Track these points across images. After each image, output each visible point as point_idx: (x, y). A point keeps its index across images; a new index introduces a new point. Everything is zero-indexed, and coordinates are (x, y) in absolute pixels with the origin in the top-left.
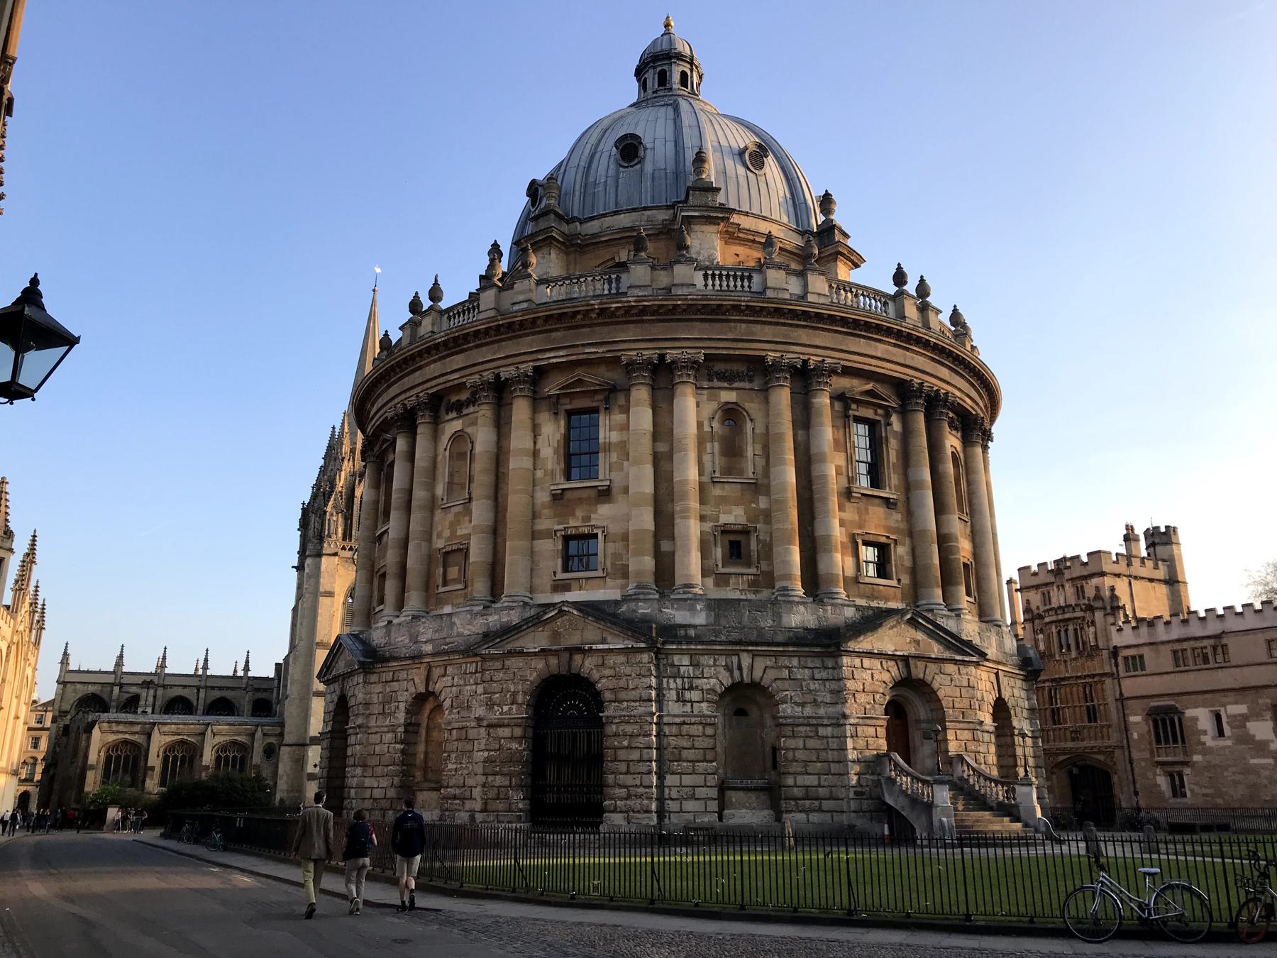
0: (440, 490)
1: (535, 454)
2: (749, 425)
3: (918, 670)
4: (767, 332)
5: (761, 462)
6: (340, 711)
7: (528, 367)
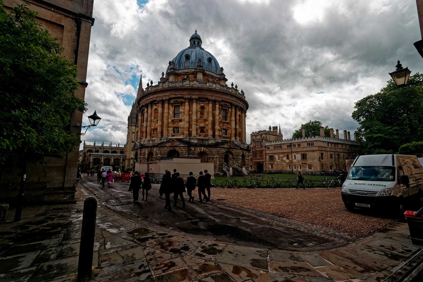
0: (152, 118)
1: (169, 113)
2: (205, 110)
4: (209, 94)
5: (207, 116)
6: (136, 154)
7: (167, 98)
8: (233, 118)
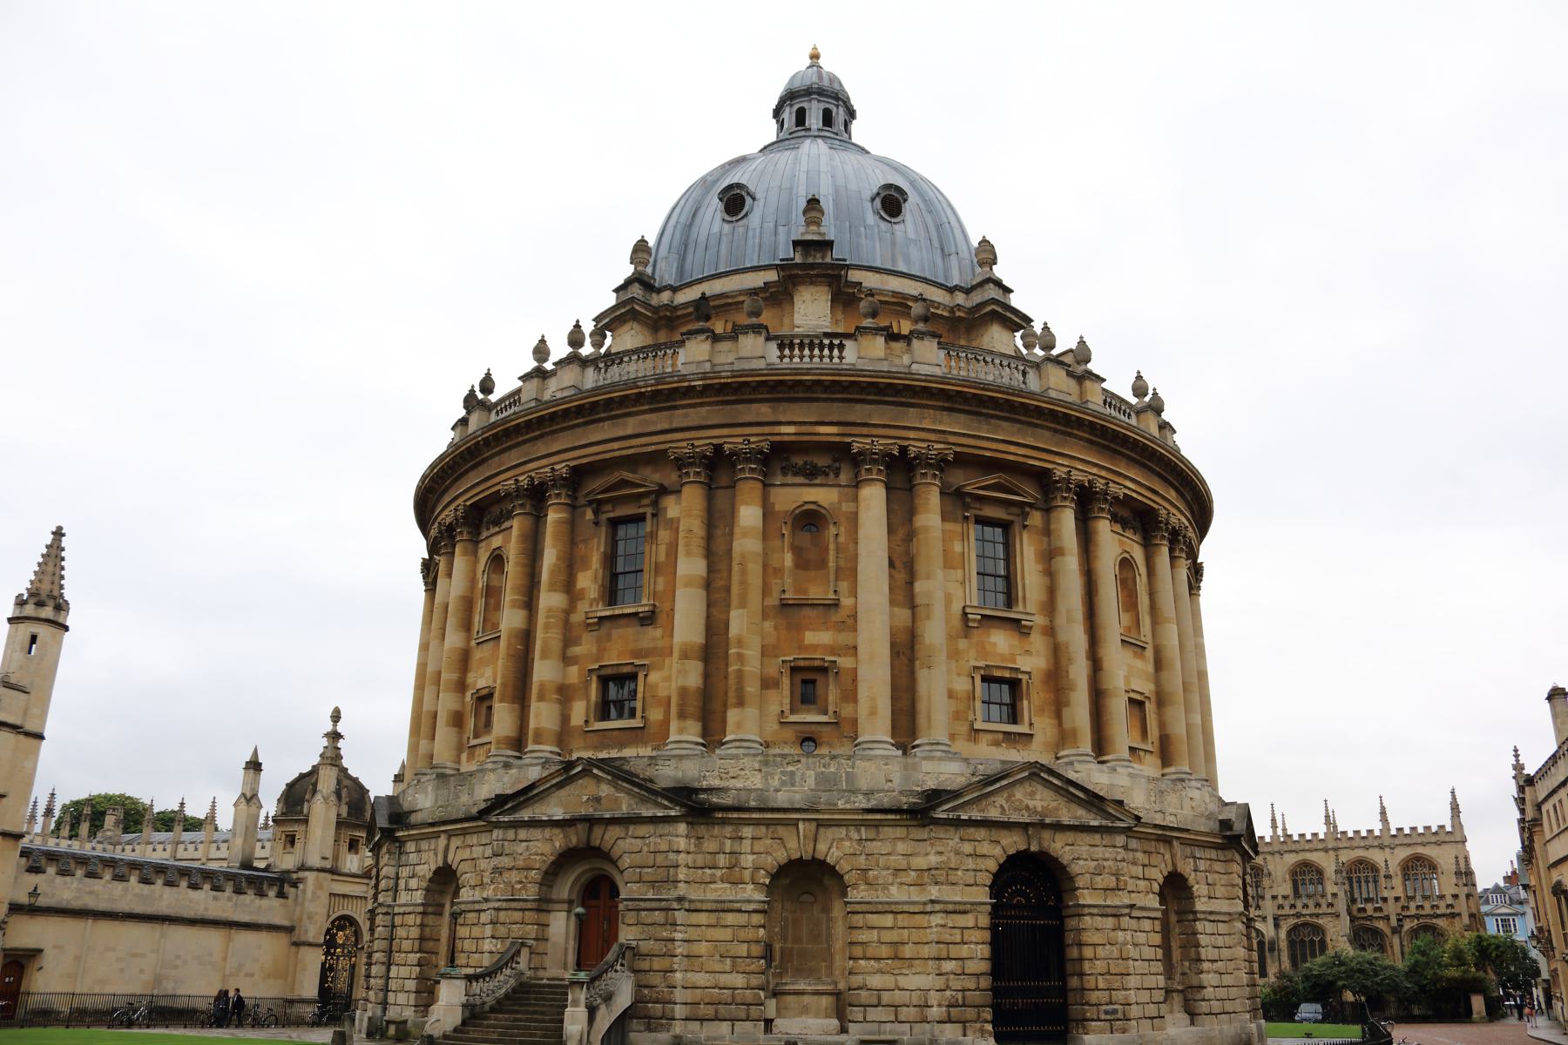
3: (598, 836)
8: (691, 566)
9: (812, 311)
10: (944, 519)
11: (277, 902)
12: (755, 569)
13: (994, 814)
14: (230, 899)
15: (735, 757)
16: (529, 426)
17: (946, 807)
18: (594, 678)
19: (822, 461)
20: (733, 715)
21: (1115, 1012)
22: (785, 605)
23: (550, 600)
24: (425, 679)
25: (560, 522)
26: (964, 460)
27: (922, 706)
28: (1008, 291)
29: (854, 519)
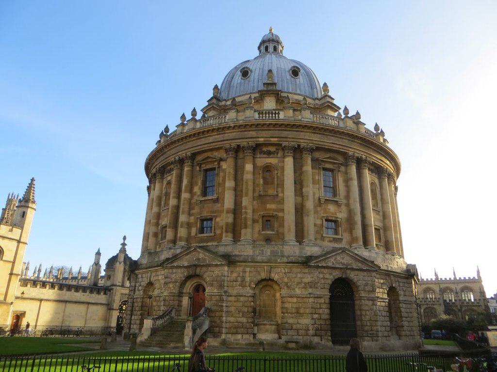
8: (230, 184)
9: (270, 104)
10: (312, 168)
11: (104, 296)
12: (251, 184)
13: (330, 264)
14: (88, 295)
15: (244, 245)
16: (178, 140)
17: (313, 262)
18: (199, 220)
19: (272, 149)
20: (243, 231)
21: (373, 334)
22: (260, 195)
23: (185, 195)
24: (148, 223)
25: (188, 170)
26: (318, 149)
27: (306, 229)
28: (333, 99)
29: (283, 168)
